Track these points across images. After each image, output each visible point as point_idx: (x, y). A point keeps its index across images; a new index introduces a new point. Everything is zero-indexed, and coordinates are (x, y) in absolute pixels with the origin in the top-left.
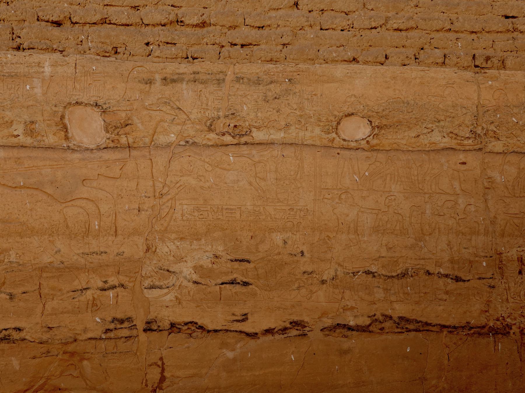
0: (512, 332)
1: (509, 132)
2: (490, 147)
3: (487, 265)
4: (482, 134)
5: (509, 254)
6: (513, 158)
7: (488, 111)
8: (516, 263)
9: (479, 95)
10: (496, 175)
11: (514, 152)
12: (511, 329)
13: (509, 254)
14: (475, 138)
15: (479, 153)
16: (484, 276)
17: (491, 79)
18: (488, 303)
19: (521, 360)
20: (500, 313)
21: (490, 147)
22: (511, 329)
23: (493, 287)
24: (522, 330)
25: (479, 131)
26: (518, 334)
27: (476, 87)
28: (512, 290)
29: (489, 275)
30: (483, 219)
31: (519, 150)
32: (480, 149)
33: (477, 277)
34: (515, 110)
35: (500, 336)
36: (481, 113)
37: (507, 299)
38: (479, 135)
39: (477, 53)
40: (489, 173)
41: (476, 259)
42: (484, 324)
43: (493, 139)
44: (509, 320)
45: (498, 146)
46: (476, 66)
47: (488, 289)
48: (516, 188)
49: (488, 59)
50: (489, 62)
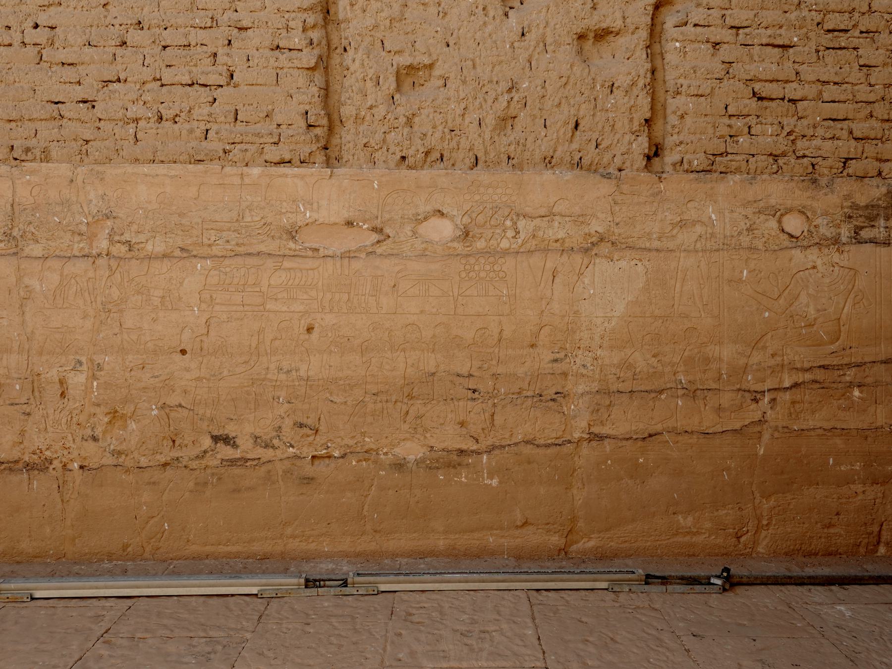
0: (51, 467)
1: (50, 234)
2: (27, 251)
3: (22, 389)
4: (18, 237)
5: (48, 375)
6: (55, 264)
7: (25, 209)
8: (58, 386)
9: (14, 192)
10: (35, 284)
11: (56, 256)
12: (51, 463)
13: (48, 375)
14: (9, 241)
15: (14, 258)
16: (17, 401)
17: (32, 173)
18: (22, 433)
19: (62, 501)
20: (37, 444)
21: (27, 251)
22: (51, 463)
23: (29, 414)
24: (65, 465)
25: (15, 233)
26: (60, 469)
27: (11, 183)
28: (51, 417)
29: (24, 400)
30: (18, 335)
31: (62, 253)
32: (15, 254)
33: (8, 402)
34: (58, 209)
35: (36, 472)
36: (17, 214)
37: (46, 429)
38: (14, 237)
39: (16, 144)
40: (26, 280)
41: (8, 381)
42: (16, 458)
43: (31, 242)
44: (48, 453)
45: (37, 250)
46: (16, 159)
47: (22, 417)
48: (58, 297)
49: (27, 150)
50: (29, 154)
